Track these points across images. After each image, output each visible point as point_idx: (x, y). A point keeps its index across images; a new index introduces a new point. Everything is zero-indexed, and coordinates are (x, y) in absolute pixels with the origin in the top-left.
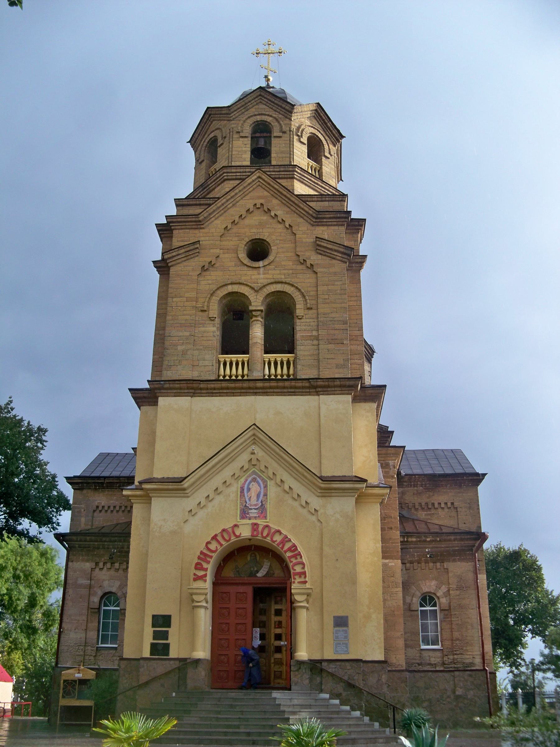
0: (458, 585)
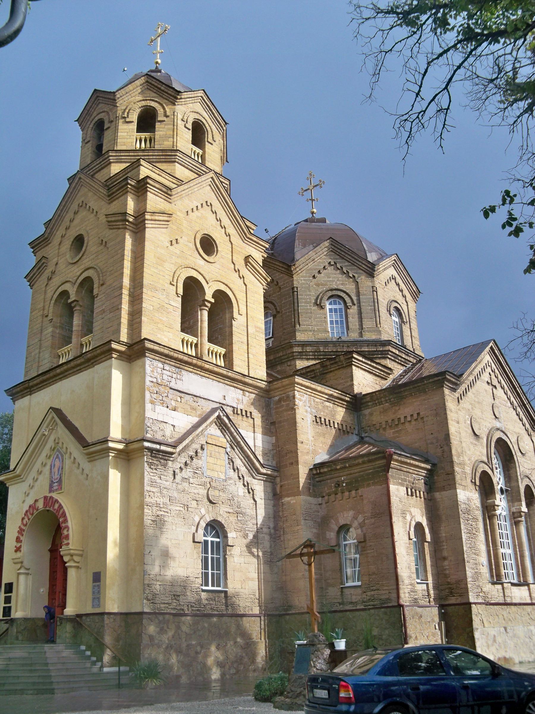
0: (372, 513)
